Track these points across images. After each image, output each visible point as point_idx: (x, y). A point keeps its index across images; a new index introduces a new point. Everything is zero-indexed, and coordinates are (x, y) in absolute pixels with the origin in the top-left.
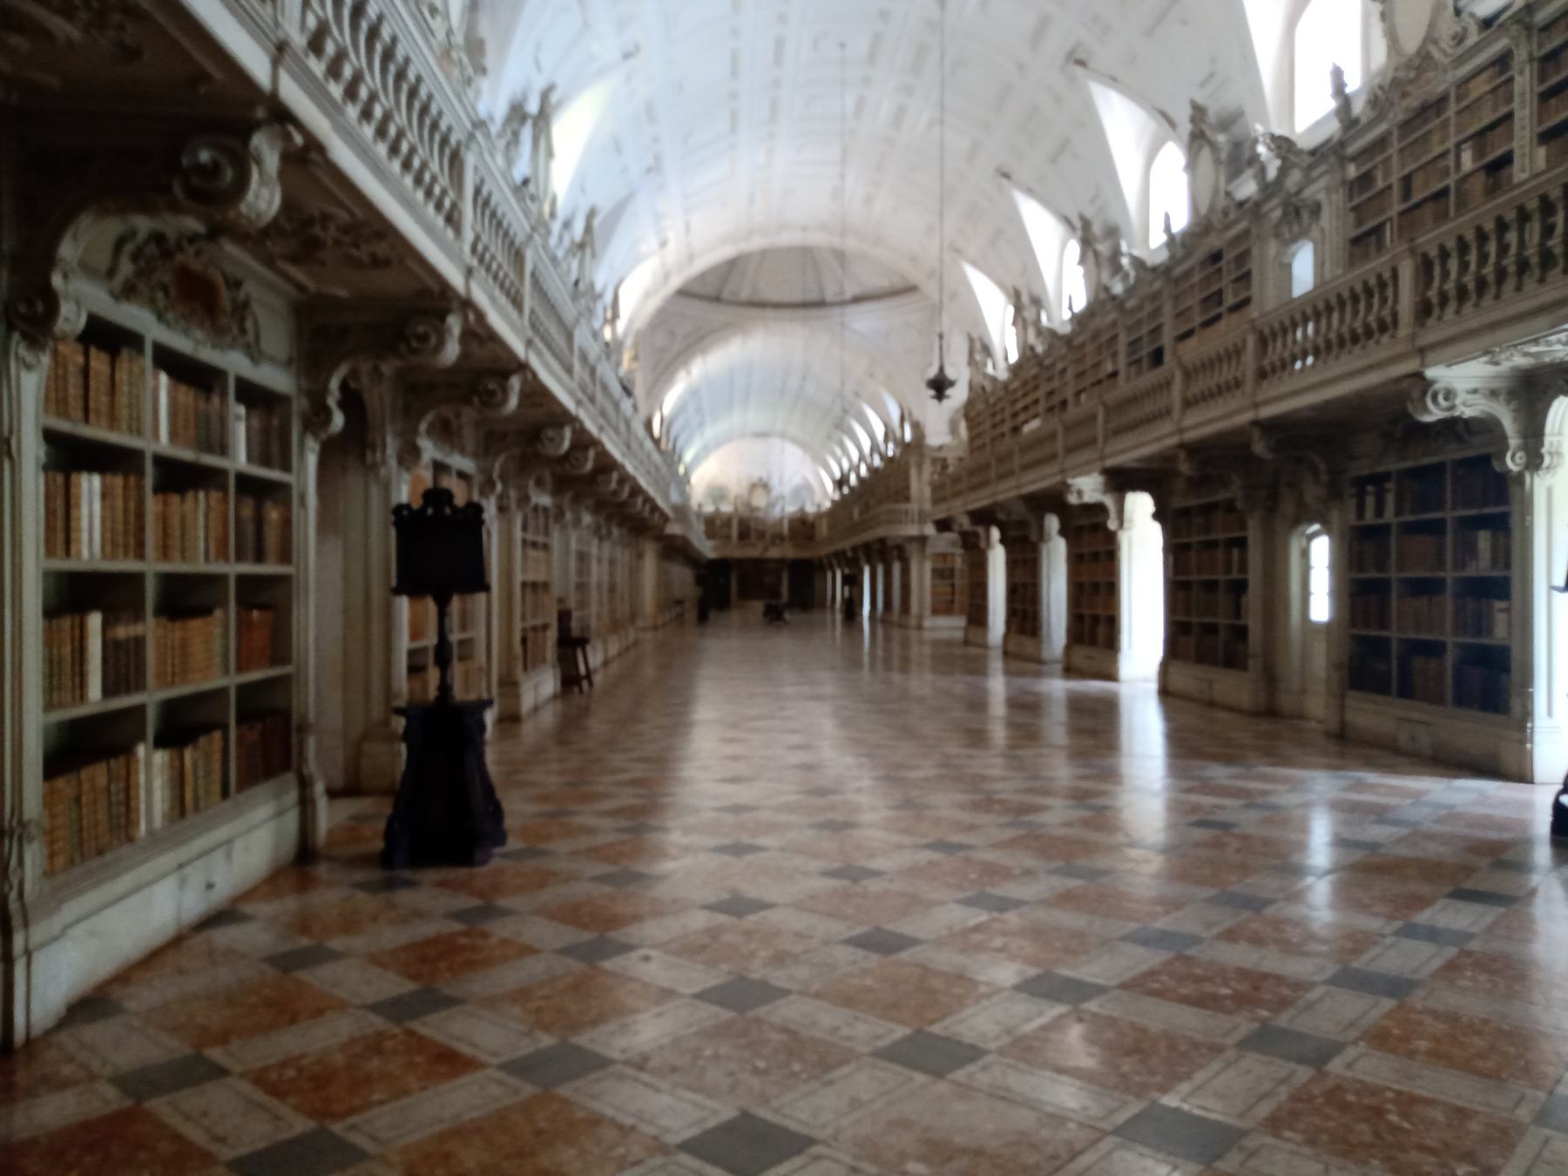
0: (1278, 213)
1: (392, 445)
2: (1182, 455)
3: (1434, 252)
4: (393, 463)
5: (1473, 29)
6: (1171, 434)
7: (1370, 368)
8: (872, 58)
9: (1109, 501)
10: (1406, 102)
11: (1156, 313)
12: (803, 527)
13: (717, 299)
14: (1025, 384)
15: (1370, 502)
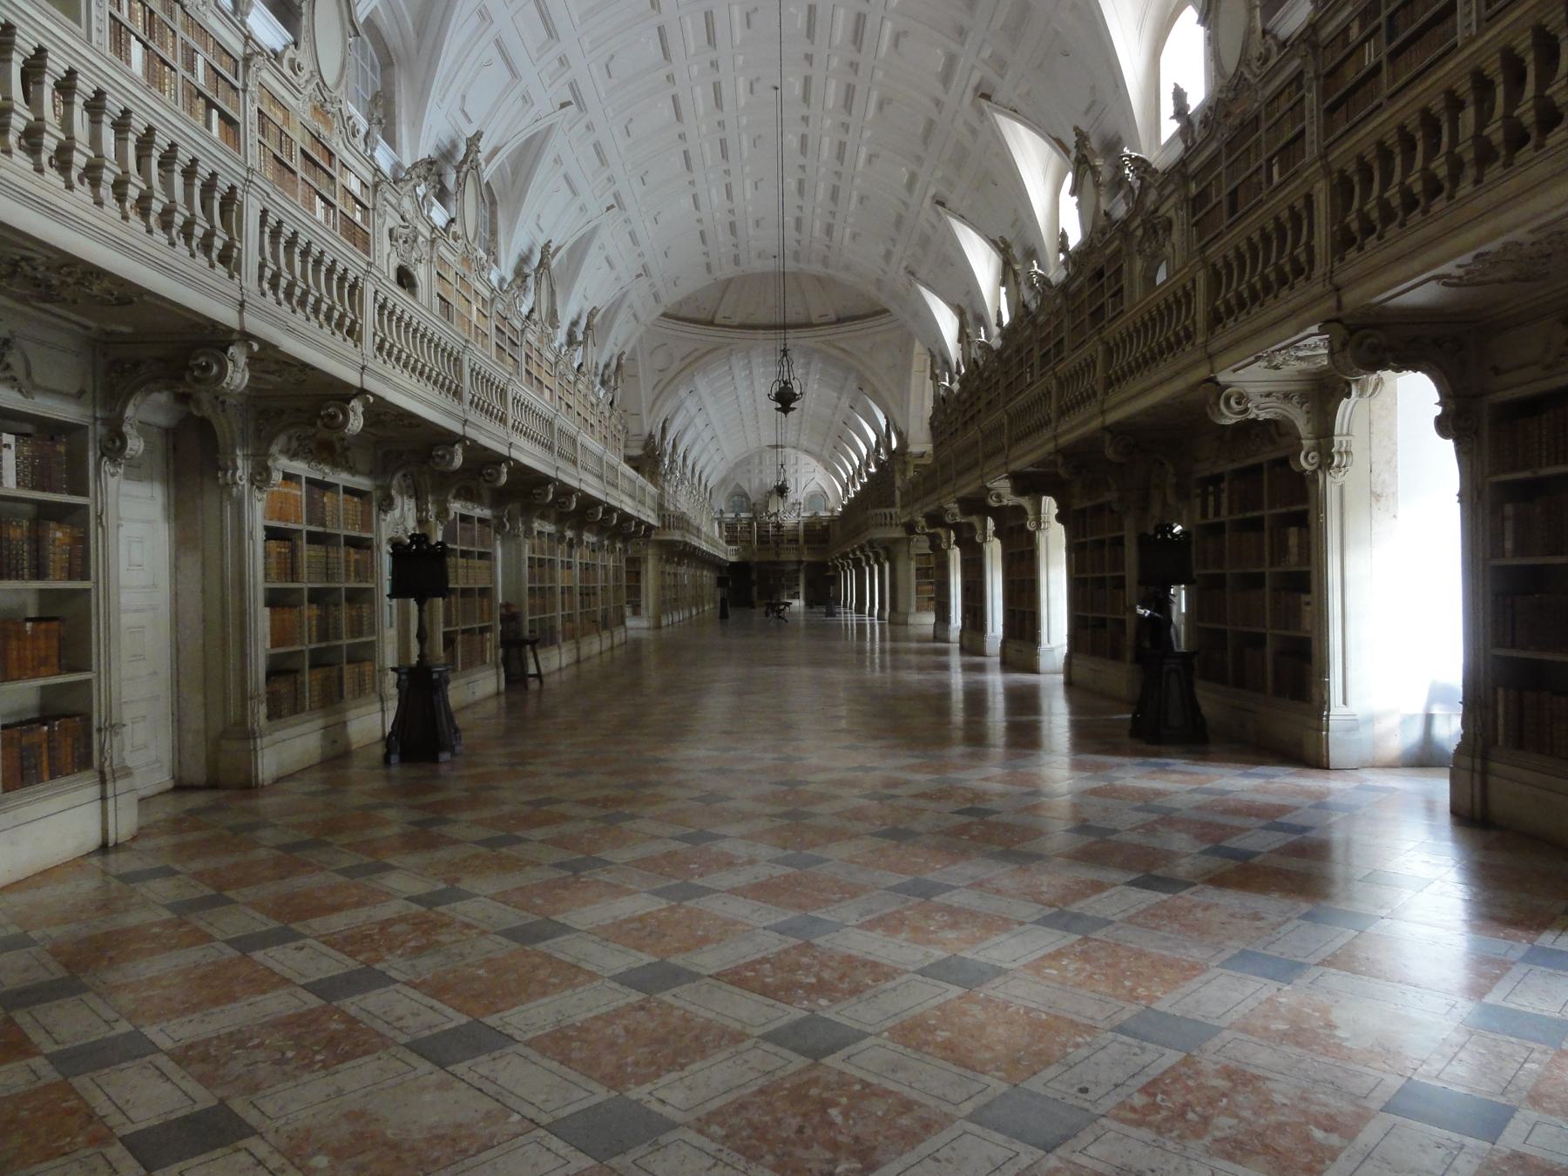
0: (1139, 232)
1: (243, 469)
2: (1060, 460)
3: (1220, 264)
5: (1275, 49)
7: (1178, 374)
8: (806, 97)
9: (1025, 502)
10: (1230, 120)
11: (1058, 328)
12: (818, 533)
13: (711, 323)
15: (1211, 499)
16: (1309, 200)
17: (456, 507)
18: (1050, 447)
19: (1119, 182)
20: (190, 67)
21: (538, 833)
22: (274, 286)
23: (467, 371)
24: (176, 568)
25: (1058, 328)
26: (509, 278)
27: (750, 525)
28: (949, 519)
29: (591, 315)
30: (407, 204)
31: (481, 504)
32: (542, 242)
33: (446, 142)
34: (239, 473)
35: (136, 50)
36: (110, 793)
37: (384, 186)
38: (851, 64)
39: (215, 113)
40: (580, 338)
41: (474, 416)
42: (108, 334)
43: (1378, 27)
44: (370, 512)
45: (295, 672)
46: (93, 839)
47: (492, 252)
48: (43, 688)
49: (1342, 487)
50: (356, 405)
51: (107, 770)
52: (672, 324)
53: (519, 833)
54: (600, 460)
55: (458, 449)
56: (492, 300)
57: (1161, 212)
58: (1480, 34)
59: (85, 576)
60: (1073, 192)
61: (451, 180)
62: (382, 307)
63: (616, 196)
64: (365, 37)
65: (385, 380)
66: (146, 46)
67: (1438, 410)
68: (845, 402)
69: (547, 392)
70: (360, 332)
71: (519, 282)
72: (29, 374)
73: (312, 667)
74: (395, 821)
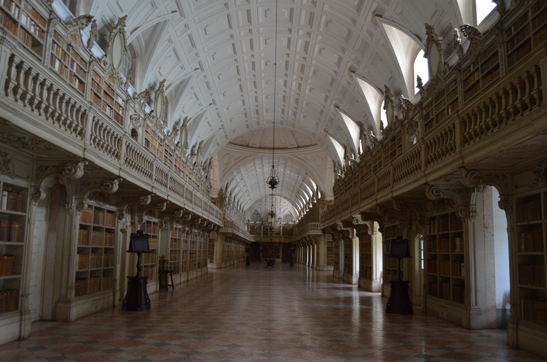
0: (407, 125)
1: (74, 203)
2: (378, 208)
3: (429, 143)
4: (74, 208)
5: (448, 70)
6: (373, 201)
7: (416, 181)
8: (287, 68)
9: (368, 223)
11: (380, 157)
12: (288, 231)
13: (248, 146)
14: (349, 179)
15: (432, 225)
16: (454, 124)
17: (146, 218)
18: (374, 203)
19: (400, 107)
20: (72, 67)
21: (174, 342)
22: (94, 141)
23: (155, 168)
24: (47, 238)
25: (380, 157)
26: (171, 130)
27: (260, 226)
28: (339, 229)
29: (201, 143)
30: (137, 106)
31: (155, 217)
32: (184, 117)
33: (152, 83)
34: (73, 205)
35: (57, 63)
36: (23, 319)
37: (130, 101)
38: (304, 58)
39: (77, 80)
40: (196, 152)
41: (156, 185)
42: (39, 157)
43: (478, 69)
44: (115, 219)
45: (86, 279)
46: (16, 335)
47: (165, 122)
48: (4, 280)
49: (474, 224)
50: (116, 182)
51: (23, 310)
52: (232, 146)
53: (167, 342)
54: (201, 200)
55: (149, 197)
56: (164, 139)
57: (414, 119)
58: (506, 76)
59: (22, 241)
60: (384, 108)
61: (153, 96)
62: (128, 146)
63: (213, 100)
64: (129, 51)
65: (127, 173)
66: (60, 61)
67: (499, 199)
68: (300, 179)
69: (182, 173)
70: (120, 156)
71: (174, 132)
72: (14, 172)
73: (91, 277)
74: (123, 334)
